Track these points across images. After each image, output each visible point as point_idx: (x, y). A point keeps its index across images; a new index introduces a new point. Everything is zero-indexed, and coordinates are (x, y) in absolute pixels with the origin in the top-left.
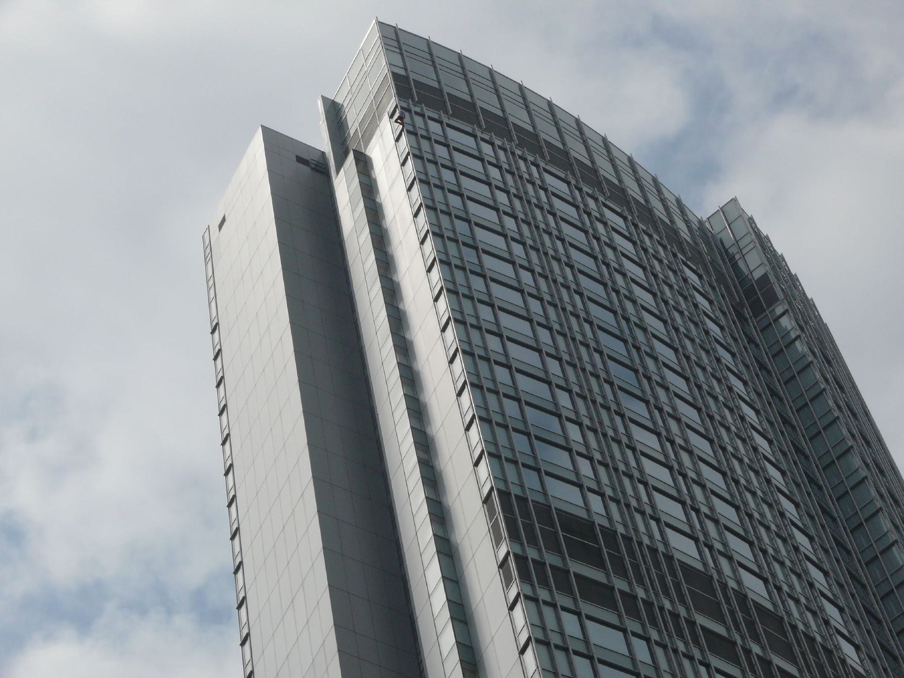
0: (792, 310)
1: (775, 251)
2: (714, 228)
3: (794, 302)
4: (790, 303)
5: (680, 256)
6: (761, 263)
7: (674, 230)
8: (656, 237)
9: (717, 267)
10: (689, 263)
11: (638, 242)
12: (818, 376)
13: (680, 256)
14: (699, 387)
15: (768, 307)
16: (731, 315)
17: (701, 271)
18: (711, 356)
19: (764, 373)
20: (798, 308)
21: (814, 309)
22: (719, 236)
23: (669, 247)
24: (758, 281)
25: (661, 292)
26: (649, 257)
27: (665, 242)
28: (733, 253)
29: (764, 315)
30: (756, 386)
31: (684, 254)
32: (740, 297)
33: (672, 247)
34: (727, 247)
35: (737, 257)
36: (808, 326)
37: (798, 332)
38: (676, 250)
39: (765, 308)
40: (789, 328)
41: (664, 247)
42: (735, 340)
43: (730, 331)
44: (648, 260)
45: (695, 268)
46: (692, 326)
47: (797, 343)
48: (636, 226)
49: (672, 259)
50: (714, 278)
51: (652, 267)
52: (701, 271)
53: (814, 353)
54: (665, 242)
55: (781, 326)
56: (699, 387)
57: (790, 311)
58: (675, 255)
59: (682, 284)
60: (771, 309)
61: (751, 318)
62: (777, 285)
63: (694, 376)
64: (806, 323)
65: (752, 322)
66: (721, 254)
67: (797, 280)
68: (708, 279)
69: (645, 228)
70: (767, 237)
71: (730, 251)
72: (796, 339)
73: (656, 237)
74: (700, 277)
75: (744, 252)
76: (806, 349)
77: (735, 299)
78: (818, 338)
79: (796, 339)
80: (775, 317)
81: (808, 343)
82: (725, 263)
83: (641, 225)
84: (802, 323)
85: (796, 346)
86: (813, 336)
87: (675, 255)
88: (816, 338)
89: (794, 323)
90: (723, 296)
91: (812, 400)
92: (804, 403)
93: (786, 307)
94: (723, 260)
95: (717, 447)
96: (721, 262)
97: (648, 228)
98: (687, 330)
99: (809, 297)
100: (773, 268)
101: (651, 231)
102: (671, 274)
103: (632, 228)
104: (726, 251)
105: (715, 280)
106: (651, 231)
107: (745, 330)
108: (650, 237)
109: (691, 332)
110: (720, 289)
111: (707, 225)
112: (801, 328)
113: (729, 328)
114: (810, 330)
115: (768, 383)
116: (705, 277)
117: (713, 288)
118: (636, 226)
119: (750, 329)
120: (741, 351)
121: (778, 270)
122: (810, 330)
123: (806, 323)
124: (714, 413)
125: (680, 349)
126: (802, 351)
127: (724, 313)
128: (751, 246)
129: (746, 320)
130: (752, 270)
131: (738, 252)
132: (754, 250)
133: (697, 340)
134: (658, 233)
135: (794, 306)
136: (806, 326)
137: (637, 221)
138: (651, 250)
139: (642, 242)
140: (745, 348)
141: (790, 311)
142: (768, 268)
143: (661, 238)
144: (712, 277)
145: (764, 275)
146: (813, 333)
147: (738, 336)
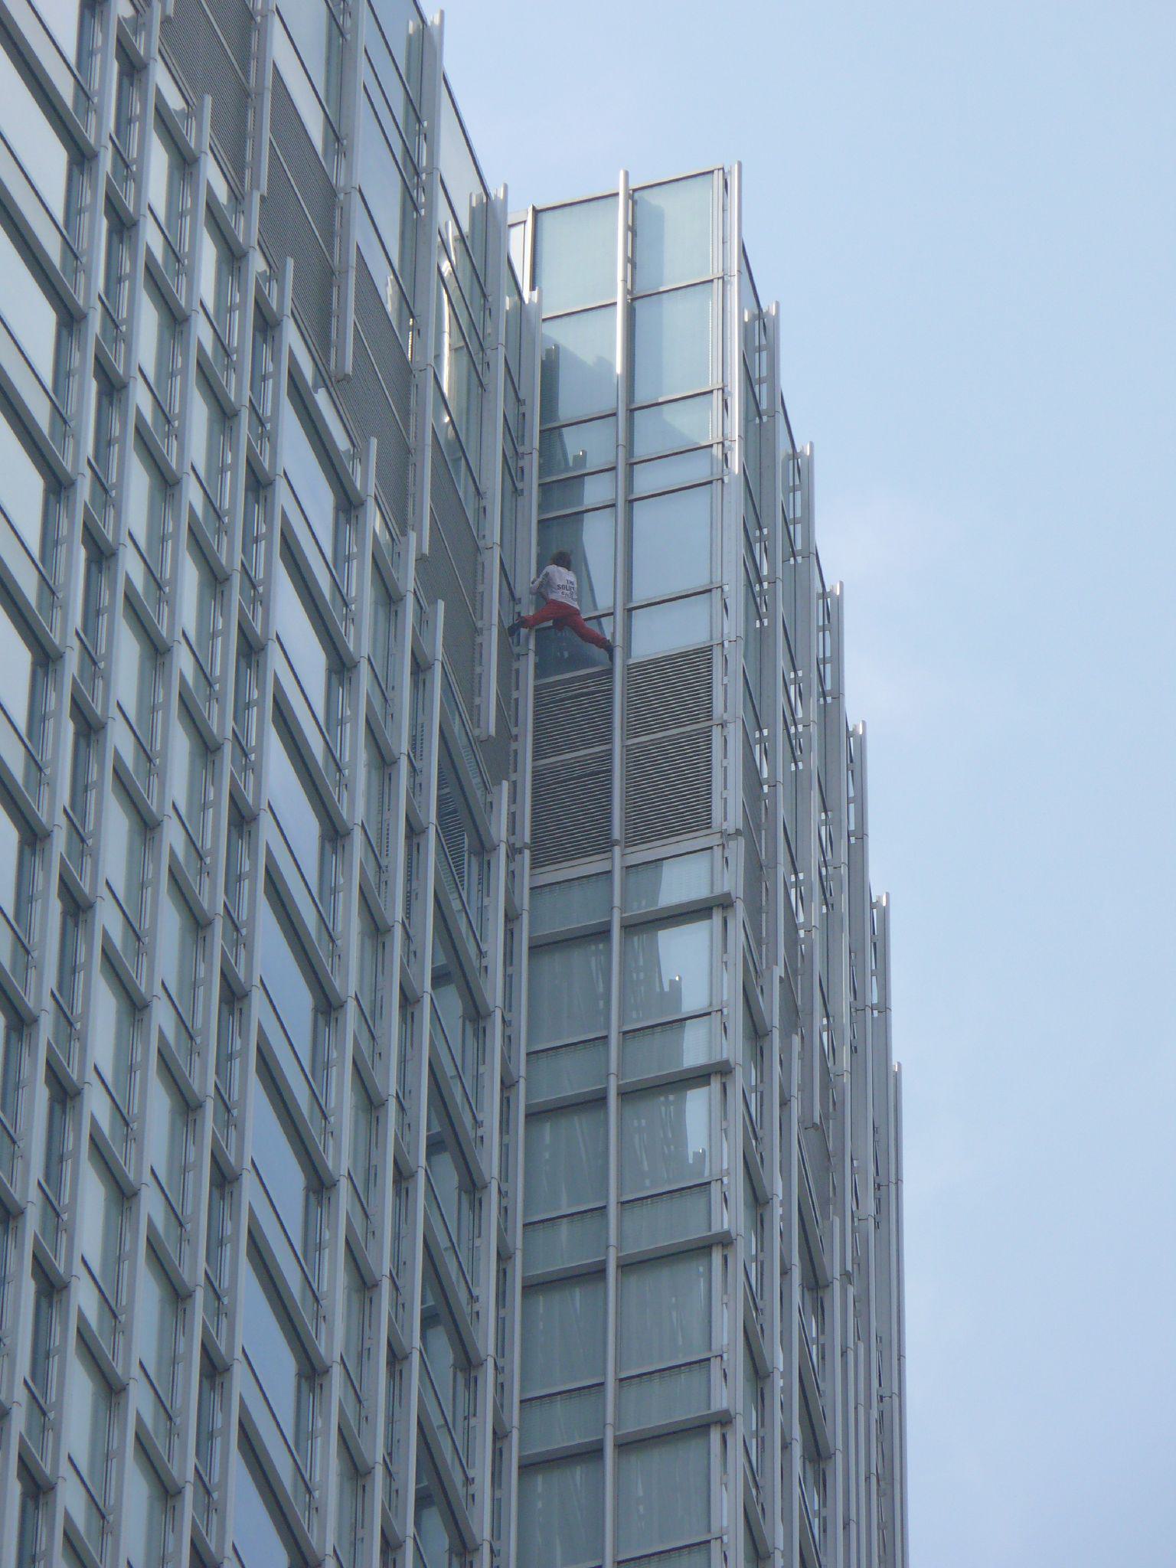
0: (755, 911)
1: (812, 554)
2: (545, 280)
3: (782, 870)
4: (757, 870)
5: (291, 337)
6: (700, 582)
7: (331, 192)
8: (212, 175)
9: (464, 487)
10: (321, 398)
11: (106, 161)
12: (727, 1332)
13: (291, 337)
14: (112, 388)
15: (637, 836)
16: (416, 787)
17: (366, 479)
18: (216, 780)
19: (452, 1003)
20: (791, 915)
21: (871, 964)
22: (558, 334)
23: (257, 264)
24: (641, 671)
25: (101, 485)
26: (116, 431)
27: (248, 229)
28: (581, 460)
29: (593, 865)
30: (364, 1418)
31: (321, 341)
32: (508, 707)
33: (275, 272)
34: (568, 408)
35: (596, 492)
36: (796, 1040)
37: (734, 1048)
38: (283, 298)
39: (617, 833)
40: (693, 1000)
41: (232, 257)
42: (376, 930)
43: (365, 1044)
44: (114, 279)
45: (342, 442)
46: (180, 746)
47: (697, 1104)
48: (133, 69)
49: (241, 330)
50: (418, 542)
51: (116, 328)
52: (366, 479)
53: (758, 1200)
54: (248, 229)
55: (654, 963)
56: (112, 388)
57: (740, 906)
58: (266, 325)
59: (233, 491)
60: (642, 854)
61: (513, 852)
62: (735, 734)
63: (90, 657)
64: (794, 1015)
65: (511, 875)
66: (514, 435)
67: (856, 764)
68: (384, 538)
69: (175, 102)
70: (800, 468)
71: (574, 443)
72: (700, 1077)
73: (212, 175)
74: (348, 505)
75: (647, 480)
76: (729, 1159)
77: (475, 712)
78: (820, 1129)
79: (700, 1077)
80: (641, 908)
81: (753, 1131)
82: (514, 491)
83: (160, 77)
84: (773, 1011)
85: (681, 1113)
86: (795, 1106)
87: (266, 325)
88: (807, 1125)
89: (731, 992)
90: (420, 668)
91: (627, 1446)
92: (585, 1259)
93: (732, 882)
94: (513, 473)
95: (59, 702)
96: (494, 480)
97: (192, 110)
98: (145, 753)
99: (880, 882)
100: (758, 642)
101: (201, 136)
102: (199, 414)
103: (108, 73)
104: (551, 434)
105: (421, 559)
106: (201, 136)
107: (456, 905)
108: (184, 163)
109: (180, 436)
110: (423, 619)
111: (519, 245)
112: (757, 1033)
113: (377, 852)
114: (796, 1065)
115: (450, 1071)
116: (375, 521)
117: (389, 598)
118: (133, 69)
119: (482, 910)
120: (384, 832)
121: (782, 662)
122: (796, 1065)
123: (794, 1015)
124: (114, 712)
125: (84, 490)
126: (700, 1157)
127: (383, 761)
128: (694, 470)
129: (483, 849)
130: (640, 596)
131: (613, 505)
132: (701, 496)
133: (173, 836)
134: (236, 167)
135: (771, 893)
136: (786, 1036)
137: (149, 44)
138: (151, 238)
139: (128, 168)
140: (409, 1001)
141: (740, 906)
142: (733, 626)
143: (237, 197)
144: (413, 536)
145: (697, 651)
146: (806, 1087)
147: (399, 914)
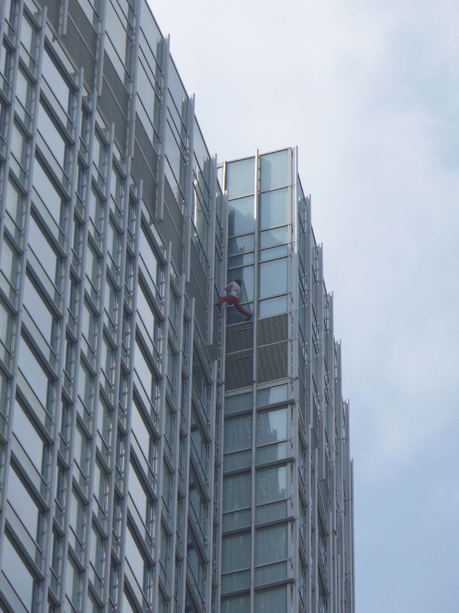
0: (303, 405)
2: (230, 187)
4: (303, 391)
5: (142, 207)
6: (284, 291)
8: (114, 150)
10: (152, 228)
13: (142, 207)
16: (185, 363)
22: (234, 205)
23: (130, 181)
27: (127, 169)
29: (246, 390)
31: (152, 208)
33: (136, 184)
34: (237, 231)
35: (247, 260)
37: (295, 453)
38: (139, 193)
39: (255, 378)
41: (122, 179)
42: (171, 412)
45: (160, 243)
48: (87, 114)
49: (125, 204)
50: (186, 277)
52: (167, 256)
53: (304, 506)
54: (127, 169)
55: (268, 424)
58: (133, 202)
60: (264, 386)
61: (219, 385)
64: (316, 442)
65: (218, 393)
66: (219, 240)
68: (174, 276)
69: (102, 125)
70: (318, 252)
71: (240, 243)
72: (283, 463)
73: (114, 150)
74: (162, 265)
75: (265, 256)
76: (294, 492)
77: (206, 337)
78: (325, 481)
79: (283, 463)
80: (262, 405)
81: (302, 482)
82: (219, 260)
83: (97, 117)
84: (309, 440)
85: (277, 476)
87: (133, 202)
90: (187, 321)
93: (295, 395)
97: (108, 128)
100: (304, 311)
101: (111, 137)
104: (232, 240)
105: (187, 283)
106: (111, 137)
108: (105, 146)
110: (187, 305)
112: (303, 448)
113: (171, 385)
117: (176, 297)
118: (87, 114)
123: (316, 442)
126: (284, 491)
128: (282, 252)
129: (209, 384)
130: (263, 296)
132: (284, 261)
141: (297, 405)
142: (295, 306)
143: (123, 158)
144: (184, 275)
147: (179, 407)
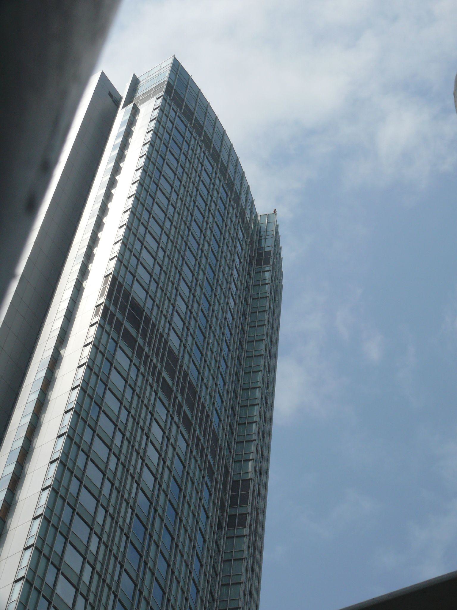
2: (261, 220)
4: (273, 268)
5: (240, 223)
9: (253, 236)
10: (242, 228)
12: (268, 304)
13: (240, 223)
22: (262, 225)
23: (238, 217)
27: (238, 215)
28: (262, 235)
33: (240, 218)
34: (261, 231)
35: (263, 238)
37: (270, 282)
38: (240, 220)
40: (267, 278)
41: (236, 217)
45: (244, 232)
47: (267, 286)
48: (230, 201)
50: (249, 240)
52: (245, 235)
53: (271, 294)
54: (238, 215)
58: (239, 222)
60: (265, 266)
61: (254, 265)
62: (272, 259)
63: (218, 275)
64: (275, 280)
66: (257, 232)
67: (282, 261)
69: (233, 204)
71: (262, 233)
72: (267, 284)
74: (244, 237)
75: (267, 237)
76: (269, 290)
77: (252, 254)
79: (267, 284)
80: (264, 270)
81: (271, 289)
82: (257, 237)
83: (232, 202)
84: (273, 279)
87: (239, 222)
93: (271, 269)
100: (275, 250)
101: (235, 207)
104: (260, 232)
106: (235, 207)
108: (233, 209)
111: (259, 218)
112: (272, 281)
113: (244, 264)
117: (246, 244)
120: (243, 276)
128: (271, 236)
129: (252, 265)
134: (237, 209)
137: (232, 200)
141: (271, 271)
142: (273, 249)
143: (237, 212)
